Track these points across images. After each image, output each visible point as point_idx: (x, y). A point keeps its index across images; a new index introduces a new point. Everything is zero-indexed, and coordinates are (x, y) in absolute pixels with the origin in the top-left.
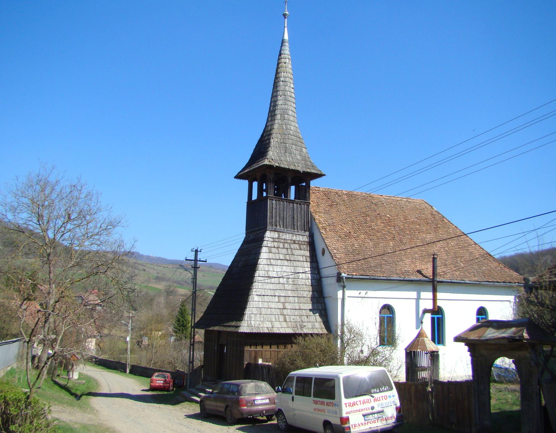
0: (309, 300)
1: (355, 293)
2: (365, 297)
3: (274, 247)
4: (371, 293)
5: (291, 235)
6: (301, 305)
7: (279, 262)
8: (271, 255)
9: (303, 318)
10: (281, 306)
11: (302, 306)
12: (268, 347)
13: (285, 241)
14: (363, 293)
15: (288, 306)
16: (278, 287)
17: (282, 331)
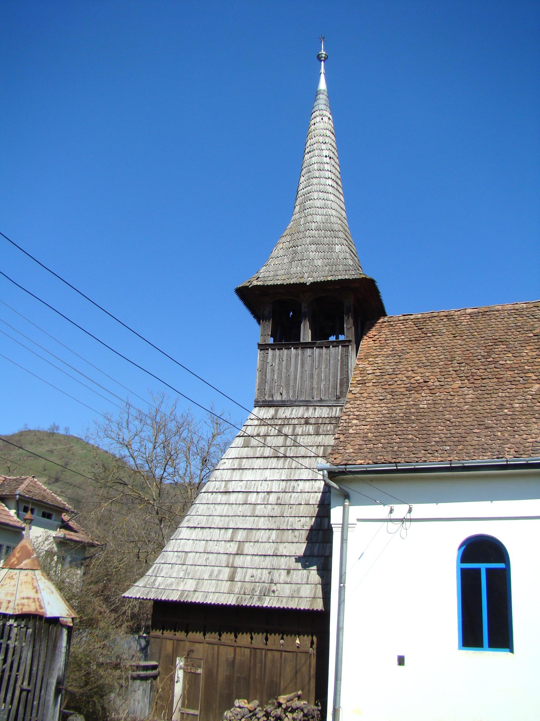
0: (305, 534)
1: (380, 511)
2: (411, 520)
3: (258, 435)
4: (421, 510)
5: (302, 409)
6: (281, 546)
7: (259, 463)
8: (245, 452)
9: (276, 573)
10: (233, 548)
11: (284, 549)
12: (232, 636)
13: (287, 422)
14: (400, 510)
15: (248, 548)
16: (240, 510)
17: (212, 599)
